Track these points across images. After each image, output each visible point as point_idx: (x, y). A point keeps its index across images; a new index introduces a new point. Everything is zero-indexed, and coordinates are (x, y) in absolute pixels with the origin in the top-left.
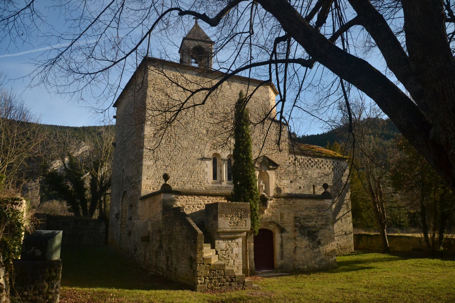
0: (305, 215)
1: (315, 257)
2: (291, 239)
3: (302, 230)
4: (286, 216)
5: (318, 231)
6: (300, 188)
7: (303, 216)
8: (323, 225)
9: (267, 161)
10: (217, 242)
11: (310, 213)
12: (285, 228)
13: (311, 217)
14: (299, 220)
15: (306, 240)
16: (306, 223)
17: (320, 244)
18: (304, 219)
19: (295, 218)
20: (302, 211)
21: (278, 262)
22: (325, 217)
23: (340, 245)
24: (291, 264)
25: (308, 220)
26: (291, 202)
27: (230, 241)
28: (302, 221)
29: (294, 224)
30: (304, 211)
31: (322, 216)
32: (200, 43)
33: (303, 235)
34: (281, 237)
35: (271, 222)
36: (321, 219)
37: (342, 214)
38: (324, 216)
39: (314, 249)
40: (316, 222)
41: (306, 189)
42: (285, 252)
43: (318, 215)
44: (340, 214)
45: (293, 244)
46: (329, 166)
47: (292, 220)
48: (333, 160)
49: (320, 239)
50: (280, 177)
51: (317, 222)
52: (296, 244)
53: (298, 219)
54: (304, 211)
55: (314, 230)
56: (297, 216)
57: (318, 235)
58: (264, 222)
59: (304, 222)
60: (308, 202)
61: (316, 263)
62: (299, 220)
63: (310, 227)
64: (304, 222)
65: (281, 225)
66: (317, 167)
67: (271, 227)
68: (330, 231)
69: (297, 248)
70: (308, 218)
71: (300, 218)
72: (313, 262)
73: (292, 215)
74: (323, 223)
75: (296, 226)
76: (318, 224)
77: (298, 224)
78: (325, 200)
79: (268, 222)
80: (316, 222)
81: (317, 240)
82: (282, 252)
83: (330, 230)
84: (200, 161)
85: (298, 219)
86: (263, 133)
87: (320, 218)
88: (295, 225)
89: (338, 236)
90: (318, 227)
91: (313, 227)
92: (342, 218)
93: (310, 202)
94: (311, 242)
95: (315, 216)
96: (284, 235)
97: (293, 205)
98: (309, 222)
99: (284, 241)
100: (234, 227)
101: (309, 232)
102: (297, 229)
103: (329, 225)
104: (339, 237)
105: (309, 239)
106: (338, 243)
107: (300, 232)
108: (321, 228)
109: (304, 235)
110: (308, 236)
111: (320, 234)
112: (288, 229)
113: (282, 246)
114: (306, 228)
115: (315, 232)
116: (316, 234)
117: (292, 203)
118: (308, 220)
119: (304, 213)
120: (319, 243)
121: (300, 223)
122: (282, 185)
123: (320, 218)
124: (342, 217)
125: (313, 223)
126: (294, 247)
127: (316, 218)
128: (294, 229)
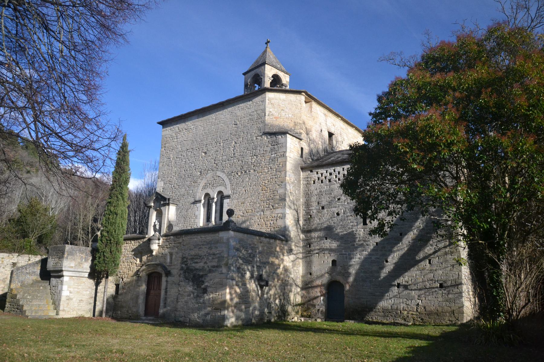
1: (199, 309)
2: (175, 284)
3: (187, 273)
4: (174, 257)
6: (338, 214)
7: (191, 255)
8: (214, 267)
9: (159, 197)
10: (52, 279)
11: (200, 252)
12: (172, 271)
13: (200, 257)
14: (186, 261)
15: (190, 286)
16: (193, 265)
18: (192, 259)
19: (183, 258)
20: (190, 249)
21: (161, 311)
22: (218, 255)
23: (425, 308)
24: (173, 315)
26: (181, 240)
27: (58, 279)
28: (189, 262)
30: (192, 249)
32: (255, 71)
33: (187, 279)
34: (167, 281)
35: (157, 265)
36: (213, 258)
37: (432, 251)
38: (217, 254)
40: (205, 263)
41: (349, 214)
43: (210, 254)
44: (429, 250)
49: (207, 286)
50: (273, 206)
54: (192, 249)
55: (201, 273)
59: (191, 264)
60: (199, 237)
61: (199, 317)
63: (197, 269)
65: (167, 267)
67: (159, 270)
71: (187, 258)
72: (196, 315)
74: (215, 264)
75: (182, 269)
76: (208, 266)
77: (184, 266)
80: (205, 263)
81: (203, 286)
82: (166, 299)
83: (222, 273)
84: (192, 205)
85: (185, 259)
86: (255, 155)
87: (211, 258)
89: (420, 290)
91: (200, 270)
92: (432, 256)
93: (201, 238)
94: (195, 289)
95: (205, 255)
96: (170, 278)
97: (182, 243)
98: (197, 263)
99: (169, 286)
100: (54, 267)
101: (194, 276)
102: (182, 272)
104: (423, 292)
105: (193, 285)
106: (418, 305)
107: (185, 276)
108: (210, 271)
109: (189, 280)
110: (193, 282)
111: (208, 279)
112: (175, 272)
114: (192, 270)
116: (203, 279)
118: (196, 261)
119: (193, 253)
120: (205, 291)
121: (186, 265)
122: (275, 217)
123: (211, 258)
124: (430, 255)
125: (202, 264)
127: (206, 258)
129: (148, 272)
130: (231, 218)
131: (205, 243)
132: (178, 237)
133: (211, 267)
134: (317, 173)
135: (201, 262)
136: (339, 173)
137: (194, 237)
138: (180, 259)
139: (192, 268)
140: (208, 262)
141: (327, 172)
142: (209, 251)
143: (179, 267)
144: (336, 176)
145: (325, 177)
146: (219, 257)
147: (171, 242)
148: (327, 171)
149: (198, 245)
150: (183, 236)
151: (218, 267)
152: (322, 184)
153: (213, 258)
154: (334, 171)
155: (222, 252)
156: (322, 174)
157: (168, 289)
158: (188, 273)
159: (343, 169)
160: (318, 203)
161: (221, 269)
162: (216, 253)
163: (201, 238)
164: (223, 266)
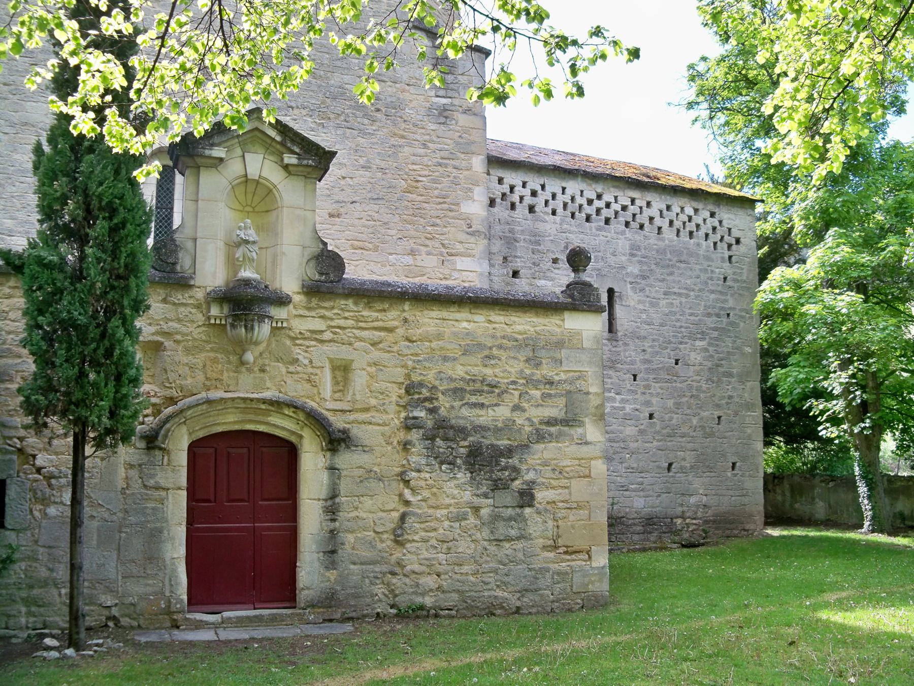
0: (462, 379)
5: (525, 447)
7: (451, 379)
8: (551, 422)
11: (488, 371)
14: (430, 399)
17: (531, 505)
18: (457, 392)
20: (445, 359)
24: (380, 590)
25: (473, 399)
28: (444, 403)
29: (403, 415)
30: (455, 359)
31: (551, 383)
33: (442, 463)
34: (332, 468)
35: (277, 405)
36: (545, 396)
38: (559, 382)
39: (501, 524)
40: (516, 408)
42: (350, 538)
43: (531, 382)
45: (393, 502)
46: (678, 224)
47: (394, 398)
48: (696, 205)
49: (534, 482)
51: (524, 411)
52: (407, 503)
53: (425, 393)
54: (455, 359)
55: (503, 443)
56: (416, 378)
57: (524, 467)
58: (244, 399)
62: (426, 399)
64: (452, 407)
66: (627, 224)
68: (585, 448)
69: (410, 520)
70: (474, 392)
73: (399, 374)
75: (410, 425)
76: (529, 419)
77: (422, 414)
78: (567, 315)
79: (264, 401)
83: (587, 443)
88: (406, 418)
90: (528, 429)
91: (497, 430)
93: (490, 322)
94: (486, 496)
95: (514, 383)
96: (346, 459)
97: (400, 331)
99: (344, 486)
103: (581, 424)
108: (540, 437)
113: (332, 510)
114: (462, 432)
115: (509, 452)
116: (514, 461)
117: (396, 323)
118: (473, 399)
119: (459, 371)
121: (433, 411)
123: (536, 393)
125: (503, 412)
126: (396, 515)
127: (516, 393)
128: (402, 435)
129: (201, 434)
130: (585, 277)
131: (510, 344)
132: (378, 306)
133: (540, 424)
134: (500, 181)
135: (497, 405)
136: (554, 196)
137: (458, 316)
138: (396, 393)
139: (462, 422)
140: (525, 405)
141: (524, 185)
142: (528, 372)
143: (394, 418)
144: (547, 202)
145: (522, 198)
146: (569, 392)
147: (342, 323)
148: (564, 189)
149: (481, 347)
150: (406, 307)
151: (570, 421)
152: (512, 213)
153: (545, 396)
154: (543, 187)
155: (578, 378)
156: (512, 188)
157: (342, 499)
158: (446, 439)
159: (564, 189)
160: (505, 258)
161: (580, 430)
162: (557, 378)
163: (490, 322)
164: (587, 420)
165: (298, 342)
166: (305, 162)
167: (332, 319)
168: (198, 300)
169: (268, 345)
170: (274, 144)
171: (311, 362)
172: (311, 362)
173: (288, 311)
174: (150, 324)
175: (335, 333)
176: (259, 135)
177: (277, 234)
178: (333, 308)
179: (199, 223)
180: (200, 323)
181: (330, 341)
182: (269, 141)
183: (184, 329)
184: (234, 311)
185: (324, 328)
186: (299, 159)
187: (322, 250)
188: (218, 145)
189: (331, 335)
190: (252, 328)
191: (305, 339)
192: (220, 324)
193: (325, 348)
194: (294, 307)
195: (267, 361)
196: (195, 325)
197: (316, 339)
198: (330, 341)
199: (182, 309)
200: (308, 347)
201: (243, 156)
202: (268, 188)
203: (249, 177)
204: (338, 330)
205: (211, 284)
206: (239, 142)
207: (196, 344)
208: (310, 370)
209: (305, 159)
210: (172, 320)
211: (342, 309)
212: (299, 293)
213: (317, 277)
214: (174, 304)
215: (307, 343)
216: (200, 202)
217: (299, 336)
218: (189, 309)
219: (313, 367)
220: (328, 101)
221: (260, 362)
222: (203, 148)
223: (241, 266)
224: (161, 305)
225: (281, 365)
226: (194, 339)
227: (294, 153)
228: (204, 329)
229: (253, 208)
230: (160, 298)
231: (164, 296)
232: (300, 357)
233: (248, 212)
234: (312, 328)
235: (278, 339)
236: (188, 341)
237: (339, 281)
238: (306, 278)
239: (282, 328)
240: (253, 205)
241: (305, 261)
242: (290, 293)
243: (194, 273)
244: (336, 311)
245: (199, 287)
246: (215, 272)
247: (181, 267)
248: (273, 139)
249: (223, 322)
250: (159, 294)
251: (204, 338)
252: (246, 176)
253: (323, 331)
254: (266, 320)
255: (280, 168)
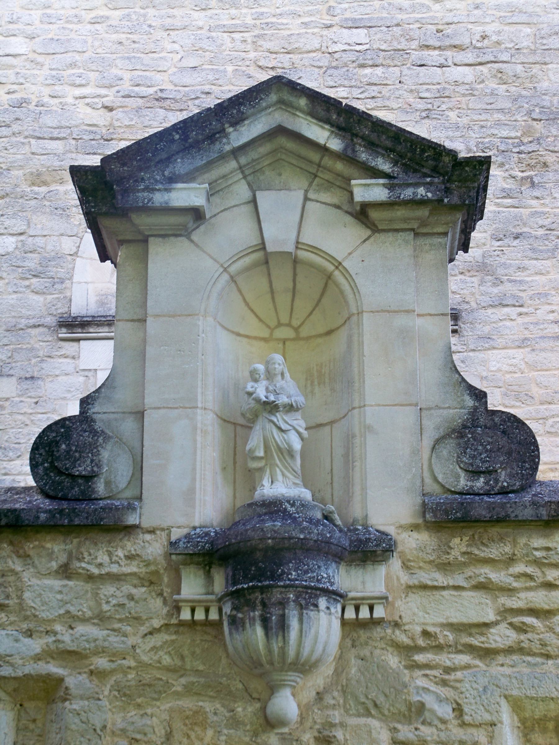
165: (420, 658)
166: (408, 193)
167: (510, 591)
168: (148, 564)
169: (337, 673)
170: (327, 161)
171: (459, 710)
172: (459, 710)
173: (388, 578)
174: (29, 634)
175: (521, 629)
176: (290, 145)
177: (350, 383)
178: (511, 560)
179: (149, 373)
180: (156, 623)
181: (509, 651)
182: (315, 156)
183: (114, 640)
184: (234, 583)
185: (491, 617)
186: (391, 187)
187: (474, 412)
188: (189, 177)
189: (513, 635)
190: (283, 626)
191: (439, 648)
192: (207, 623)
193: (495, 670)
194: (406, 566)
195: (336, 716)
196: (144, 629)
197: (470, 649)
198: (509, 651)
199: (108, 590)
200: (448, 670)
201: (254, 201)
202: (321, 270)
203: (270, 248)
204: (530, 620)
205: (182, 520)
206: (241, 168)
207: (147, 678)
208: (457, 733)
209: (409, 185)
210: (84, 620)
211: (537, 562)
212: (415, 527)
213: (463, 482)
214: (90, 578)
215: (445, 659)
216: (149, 320)
217: (421, 642)
218: (127, 588)
219: (463, 725)
220: (538, 126)
221: (318, 716)
222: (147, 189)
223: (261, 470)
224: (57, 583)
225: (375, 723)
226: (142, 666)
227: (375, 173)
228: (165, 637)
229: (296, 330)
230: (54, 565)
231: (63, 558)
232: (430, 701)
233: (284, 341)
234: (456, 617)
235: (366, 652)
236: (125, 671)
237: (523, 489)
238: (436, 489)
239: (373, 622)
240: (295, 323)
241: (427, 443)
242: (391, 530)
243: (140, 498)
244: (520, 568)
245: (152, 531)
246: (191, 491)
247: (108, 483)
248: (324, 149)
249: (214, 616)
250: (51, 555)
251: (167, 660)
252: (263, 246)
253: (486, 625)
254: (322, 602)
255: (349, 219)
